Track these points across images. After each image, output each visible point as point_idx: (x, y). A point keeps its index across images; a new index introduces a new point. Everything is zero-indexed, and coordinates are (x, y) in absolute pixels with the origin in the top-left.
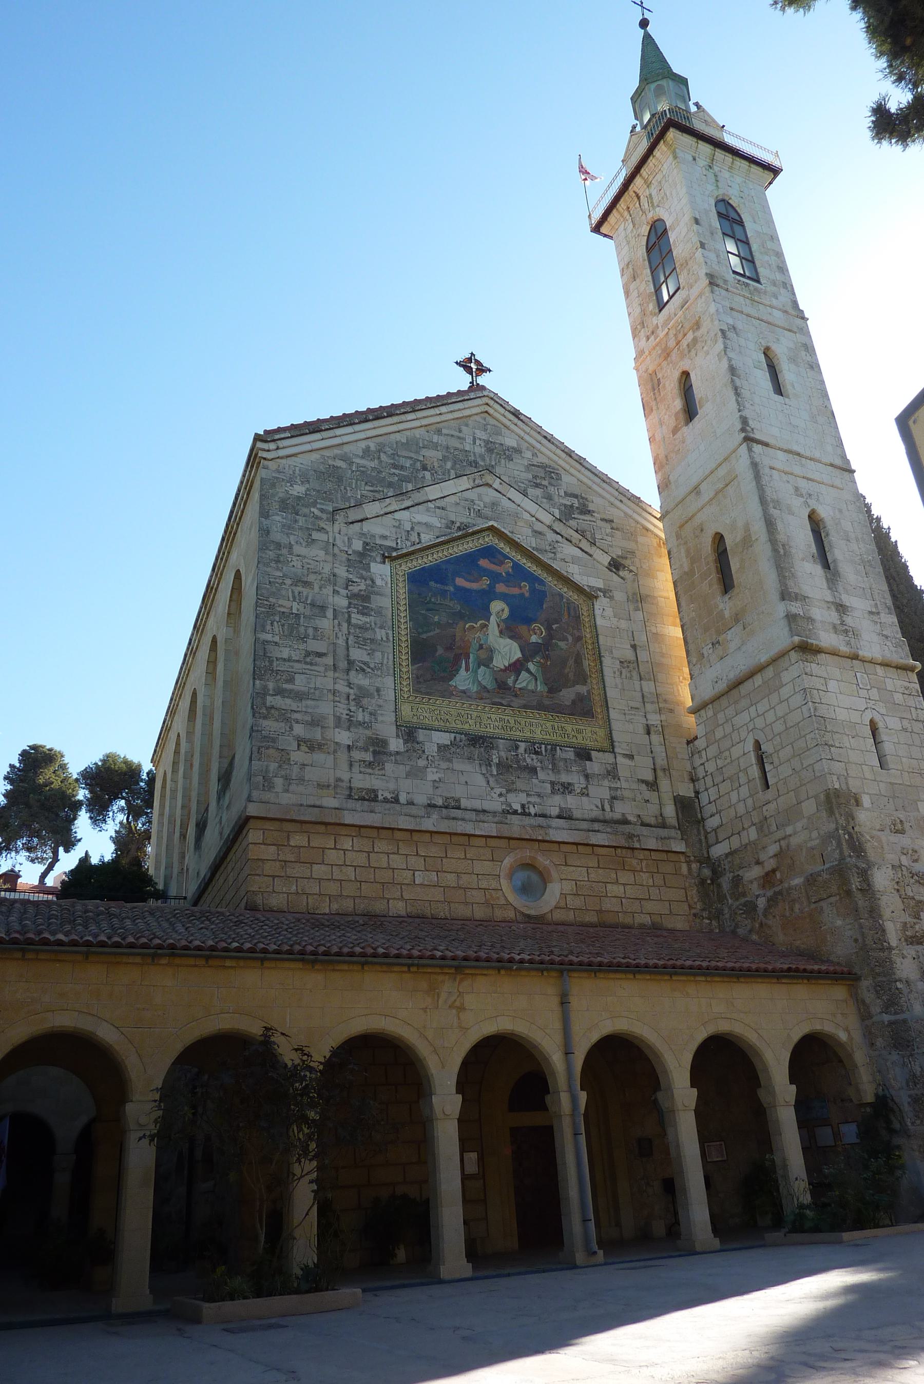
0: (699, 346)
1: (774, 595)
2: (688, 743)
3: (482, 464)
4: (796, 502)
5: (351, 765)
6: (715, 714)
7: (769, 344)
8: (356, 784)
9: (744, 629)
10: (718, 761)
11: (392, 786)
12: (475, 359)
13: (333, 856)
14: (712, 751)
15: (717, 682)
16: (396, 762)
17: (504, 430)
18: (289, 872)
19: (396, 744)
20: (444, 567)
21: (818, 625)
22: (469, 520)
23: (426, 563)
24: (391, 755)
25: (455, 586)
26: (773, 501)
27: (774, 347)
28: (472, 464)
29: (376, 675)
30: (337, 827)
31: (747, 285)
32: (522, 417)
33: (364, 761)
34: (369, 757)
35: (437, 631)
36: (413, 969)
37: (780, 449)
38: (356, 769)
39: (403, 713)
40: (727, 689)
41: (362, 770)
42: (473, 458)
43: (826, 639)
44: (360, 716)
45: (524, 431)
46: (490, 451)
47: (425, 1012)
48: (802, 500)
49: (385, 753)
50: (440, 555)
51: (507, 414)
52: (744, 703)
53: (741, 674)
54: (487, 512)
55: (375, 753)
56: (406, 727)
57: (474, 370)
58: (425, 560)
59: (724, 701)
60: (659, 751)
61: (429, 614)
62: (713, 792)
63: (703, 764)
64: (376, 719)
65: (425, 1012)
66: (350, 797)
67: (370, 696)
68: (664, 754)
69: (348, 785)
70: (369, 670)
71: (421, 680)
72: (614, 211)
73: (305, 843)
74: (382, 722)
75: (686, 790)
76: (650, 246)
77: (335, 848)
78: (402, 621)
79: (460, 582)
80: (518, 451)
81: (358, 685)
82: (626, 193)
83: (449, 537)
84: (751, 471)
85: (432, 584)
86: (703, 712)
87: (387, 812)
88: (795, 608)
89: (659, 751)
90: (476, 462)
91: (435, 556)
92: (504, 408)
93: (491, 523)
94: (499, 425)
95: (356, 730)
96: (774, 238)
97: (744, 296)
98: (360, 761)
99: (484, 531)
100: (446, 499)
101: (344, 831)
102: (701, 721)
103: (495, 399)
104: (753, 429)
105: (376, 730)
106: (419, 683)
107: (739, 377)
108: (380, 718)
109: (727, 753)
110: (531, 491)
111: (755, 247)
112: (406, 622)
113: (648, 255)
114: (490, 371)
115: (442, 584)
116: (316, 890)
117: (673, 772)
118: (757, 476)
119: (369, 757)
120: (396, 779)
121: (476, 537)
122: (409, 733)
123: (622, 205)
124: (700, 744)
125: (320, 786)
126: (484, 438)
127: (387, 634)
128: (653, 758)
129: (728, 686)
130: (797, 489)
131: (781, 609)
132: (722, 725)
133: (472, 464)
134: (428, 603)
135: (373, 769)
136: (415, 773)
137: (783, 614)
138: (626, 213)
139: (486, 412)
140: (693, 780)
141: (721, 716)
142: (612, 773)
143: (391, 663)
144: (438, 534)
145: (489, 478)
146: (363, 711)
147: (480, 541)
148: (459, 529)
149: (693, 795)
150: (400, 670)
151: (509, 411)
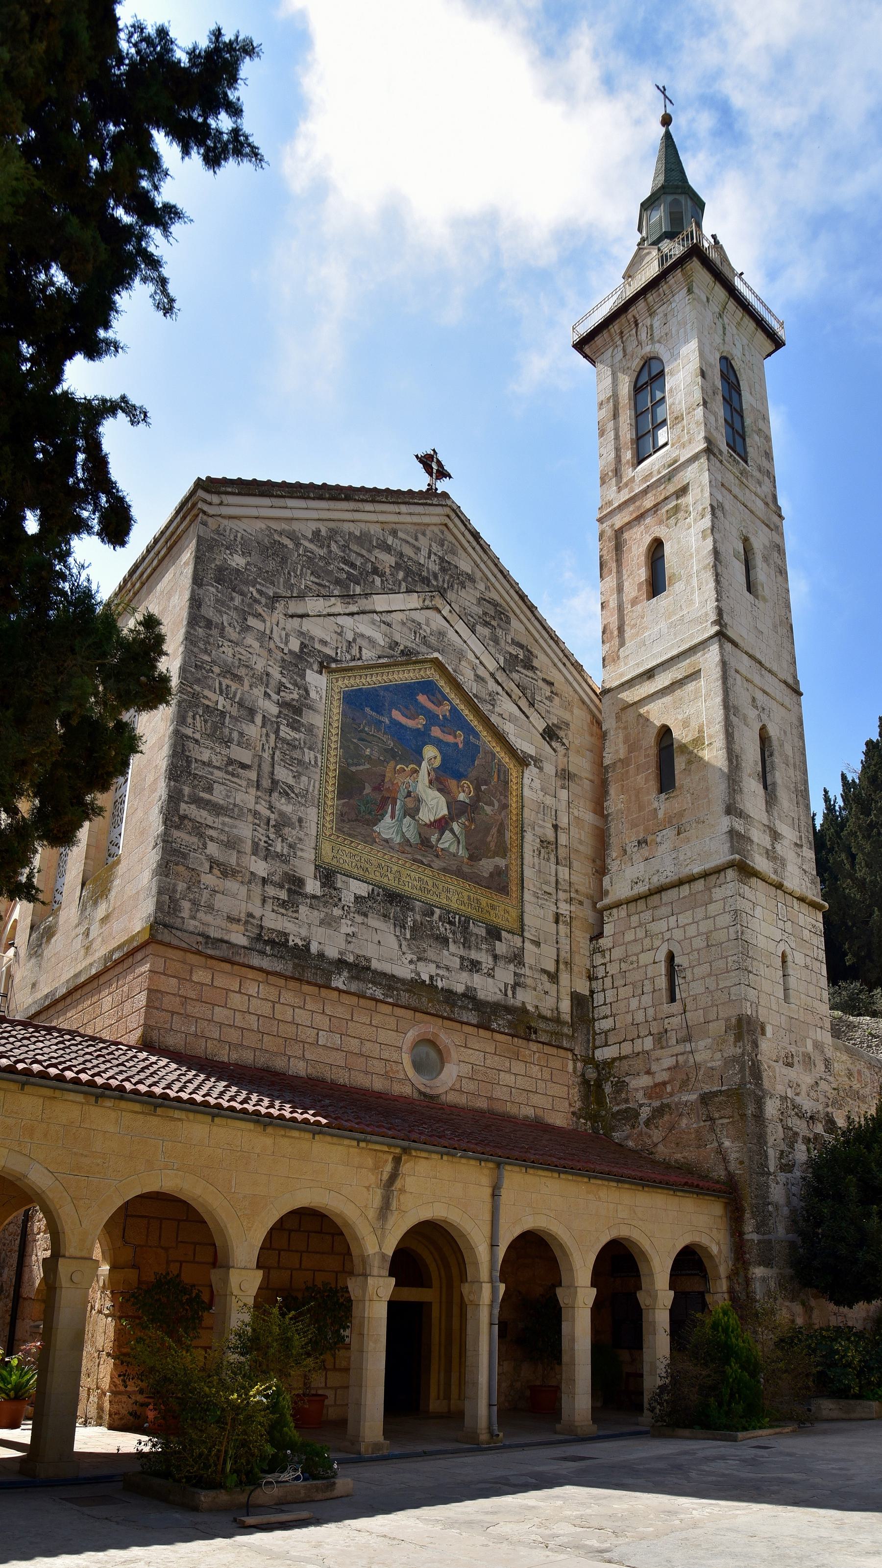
0: (681, 515)
1: (719, 807)
2: (591, 939)
3: (435, 583)
4: (752, 713)
5: (264, 901)
6: (629, 916)
7: (750, 535)
8: (267, 923)
9: (679, 834)
10: (622, 964)
11: (304, 932)
12: (437, 459)
13: (236, 1000)
14: (617, 953)
15: (636, 883)
16: (311, 907)
17: (460, 551)
18: (190, 1010)
19: (313, 886)
20: (382, 693)
21: (755, 847)
22: (414, 646)
23: (364, 685)
24: (306, 896)
25: (391, 718)
26: (734, 707)
27: (753, 539)
28: (426, 581)
29: (299, 802)
30: (244, 969)
31: (738, 463)
32: (482, 542)
33: (278, 899)
34: (283, 895)
35: (367, 766)
36: (363, 1144)
37: (746, 653)
38: (269, 906)
39: (323, 853)
40: (648, 893)
41: (276, 908)
42: (425, 574)
43: (761, 863)
44: (279, 847)
45: (481, 558)
46: (443, 570)
47: (368, 1190)
48: (757, 712)
49: (300, 894)
50: (379, 678)
51: (467, 533)
52: (664, 910)
53: (668, 880)
54: (432, 640)
55: (290, 891)
56: (325, 868)
57: (434, 471)
58: (364, 681)
59: (641, 904)
60: (564, 943)
61: (360, 744)
62: (610, 995)
63: (604, 964)
64: (295, 853)
65: (368, 1190)
66: (259, 938)
67: (291, 825)
68: (568, 947)
69: (259, 923)
70: (293, 795)
71: (345, 818)
72: (605, 333)
73: (208, 981)
74: (301, 857)
75: (582, 987)
76: (640, 384)
77: (240, 992)
78: (333, 746)
79: (396, 715)
80: (471, 579)
81: (279, 810)
82: (623, 317)
83: (392, 660)
84: (719, 669)
85: (367, 710)
86: (615, 911)
87: (296, 961)
88: (739, 825)
89: (564, 943)
90: (429, 581)
91: (374, 679)
92: (465, 525)
93: (436, 655)
94: (457, 544)
95: (273, 862)
96: (765, 418)
97: (733, 474)
98: (274, 898)
99: (427, 662)
100: (394, 615)
101: (251, 974)
102: (611, 919)
103: (457, 512)
104: (726, 624)
105: (294, 866)
106: (343, 821)
107: (720, 563)
108: (299, 853)
109: (634, 958)
110: (478, 628)
111: (748, 421)
112: (336, 748)
113: (636, 395)
114: (450, 477)
115: (378, 712)
116: (216, 1035)
117: (575, 968)
118: (725, 678)
119: (283, 895)
120: (309, 925)
121: (418, 667)
122: (327, 876)
123: (615, 328)
124: (604, 942)
125: (231, 919)
126: (439, 554)
127: (316, 757)
128: (558, 949)
129: (649, 890)
130: (754, 699)
131: (725, 823)
132: (635, 928)
133: (426, 581)
134: (360, 732)
135: (287, 910)
136: (328, 922)
137: (727, 830)
138: (617, 338)
139: (446, 525)
140: (591, 978)
141: (635, 919)
142: (517, 958)
143: (316, 792)
144: (380, 653)
145: (438, 602)
146: (283, 841)
147: (422, 673)
148: (402, 651)
149: (587, 993)
150: (325, 803)
151: (469, 531)
